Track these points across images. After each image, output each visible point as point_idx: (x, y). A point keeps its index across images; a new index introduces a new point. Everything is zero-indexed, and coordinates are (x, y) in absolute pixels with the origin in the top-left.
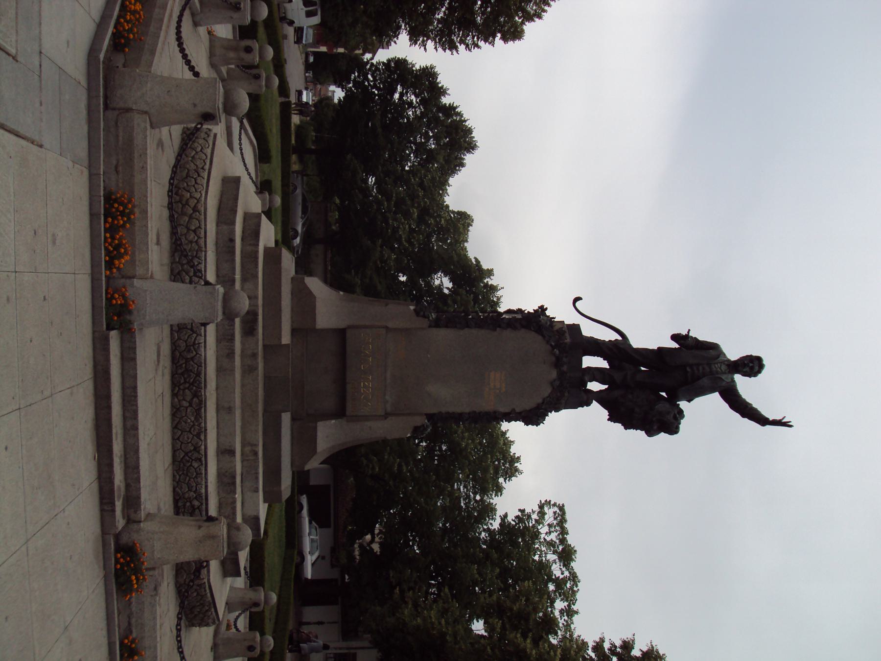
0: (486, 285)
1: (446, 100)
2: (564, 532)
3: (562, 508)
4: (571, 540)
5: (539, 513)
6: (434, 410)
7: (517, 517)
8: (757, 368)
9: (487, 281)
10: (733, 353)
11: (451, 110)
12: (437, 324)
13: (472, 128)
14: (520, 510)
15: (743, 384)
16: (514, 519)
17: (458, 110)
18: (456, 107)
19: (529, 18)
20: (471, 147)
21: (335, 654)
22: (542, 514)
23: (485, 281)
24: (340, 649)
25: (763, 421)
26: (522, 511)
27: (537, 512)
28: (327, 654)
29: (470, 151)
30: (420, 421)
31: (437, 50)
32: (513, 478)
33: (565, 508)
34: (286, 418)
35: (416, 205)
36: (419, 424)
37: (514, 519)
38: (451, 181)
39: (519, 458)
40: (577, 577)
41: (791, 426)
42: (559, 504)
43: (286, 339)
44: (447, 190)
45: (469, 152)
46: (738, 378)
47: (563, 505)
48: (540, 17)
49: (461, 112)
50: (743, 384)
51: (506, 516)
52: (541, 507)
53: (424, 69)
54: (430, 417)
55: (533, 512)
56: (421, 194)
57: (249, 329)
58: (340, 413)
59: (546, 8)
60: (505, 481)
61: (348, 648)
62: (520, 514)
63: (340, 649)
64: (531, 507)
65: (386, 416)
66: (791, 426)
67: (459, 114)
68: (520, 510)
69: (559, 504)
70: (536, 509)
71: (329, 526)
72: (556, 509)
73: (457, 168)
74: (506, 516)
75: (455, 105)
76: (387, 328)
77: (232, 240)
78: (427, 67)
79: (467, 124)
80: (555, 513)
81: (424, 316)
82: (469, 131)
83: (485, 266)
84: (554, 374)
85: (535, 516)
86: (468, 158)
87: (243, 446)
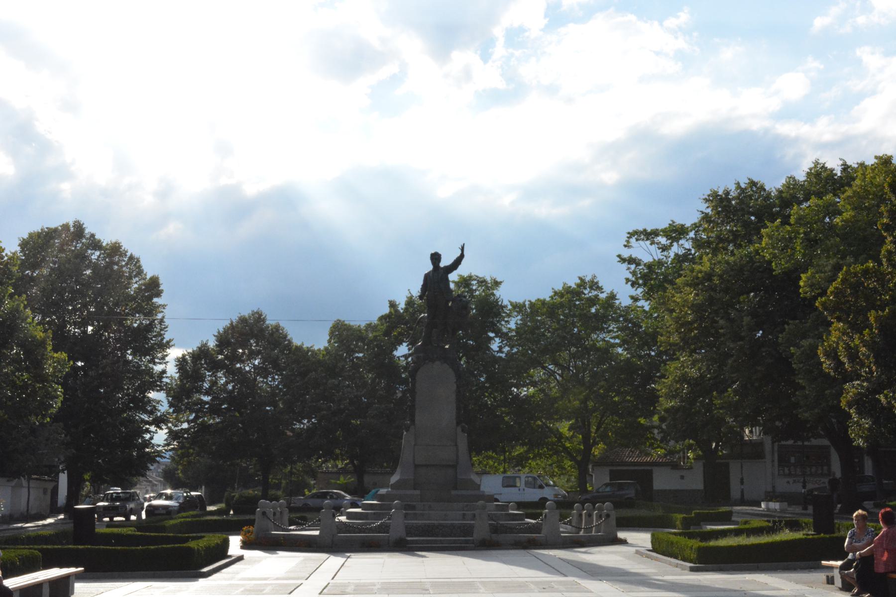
0: (406, 310)
1: (212, 344)
2: (655, 233)
3: (631, 235)
4: (663, 224)
5: (629, 263)
6: (455, 422)
7: (633, 285)
8: (437, 257)
9: (402, 309)
10: (429, 267)
11: (223, 340)
12: (413, 421)
13: (239, 316)
14: (627, 283)
15: (445, 262)
16: (635, 289)
17: (221, 330)
18: (219, 332)
19: (140, 272)
20: (259, 318)
21: (779, 466)
22: (631, 261)
23: (402, 311)
24: (773, 461)
25: (462, 256)
26: (628, 280)
27: (629, 266)
28: (779, 475)
29: (264, 318)
30: (459, 429)
31: (168, 362)
32: (600, 285)
33: (631, 231)
34: (453, 492)
35: (324, 381)
36: (460, 430)
37: (635, 289)
38: (296, 342)
39: (580, 278)
40: (695, 224)
41: (464, 244)
42: (628, 237)
43: (418, 492)
44: (307, 348)
45: (264, 320)
46: (442, 265)
47: (629, 233)
48: (138, 261)
49: (224, 329)
50: (445, 262)
51: (632, 297)
52: (623, 260)
53: (179, 369)
54: (458, 424)
55: (629, 269)
56: (313, 375)
57: (413, 508)
58: (454, 467)
59: (128, 254)
60: (603, 292)
61: (773, 454)
62: (630, 283)
63: (773, 461)
64: (624, 272)
65: (456, 445)
66: (464, 244)
67: (226, 330)
68: (627, 283)
69: (628, 237)
70: (625, 265)
71: (652, 470)
72: (633, 240)
73: (281, 332)
74: (632, 297)
75: (216, 334)
76: (415, 445)
77: (374, 513)
78: (177, 365)
79: (234, 321)
80: (637, 240)
81: (409, 428)
82: (243, 320)
83: (386, 310)
84: (438, 363)
85: (633, 267)
86: (270, 321)
87: (463, 511)
